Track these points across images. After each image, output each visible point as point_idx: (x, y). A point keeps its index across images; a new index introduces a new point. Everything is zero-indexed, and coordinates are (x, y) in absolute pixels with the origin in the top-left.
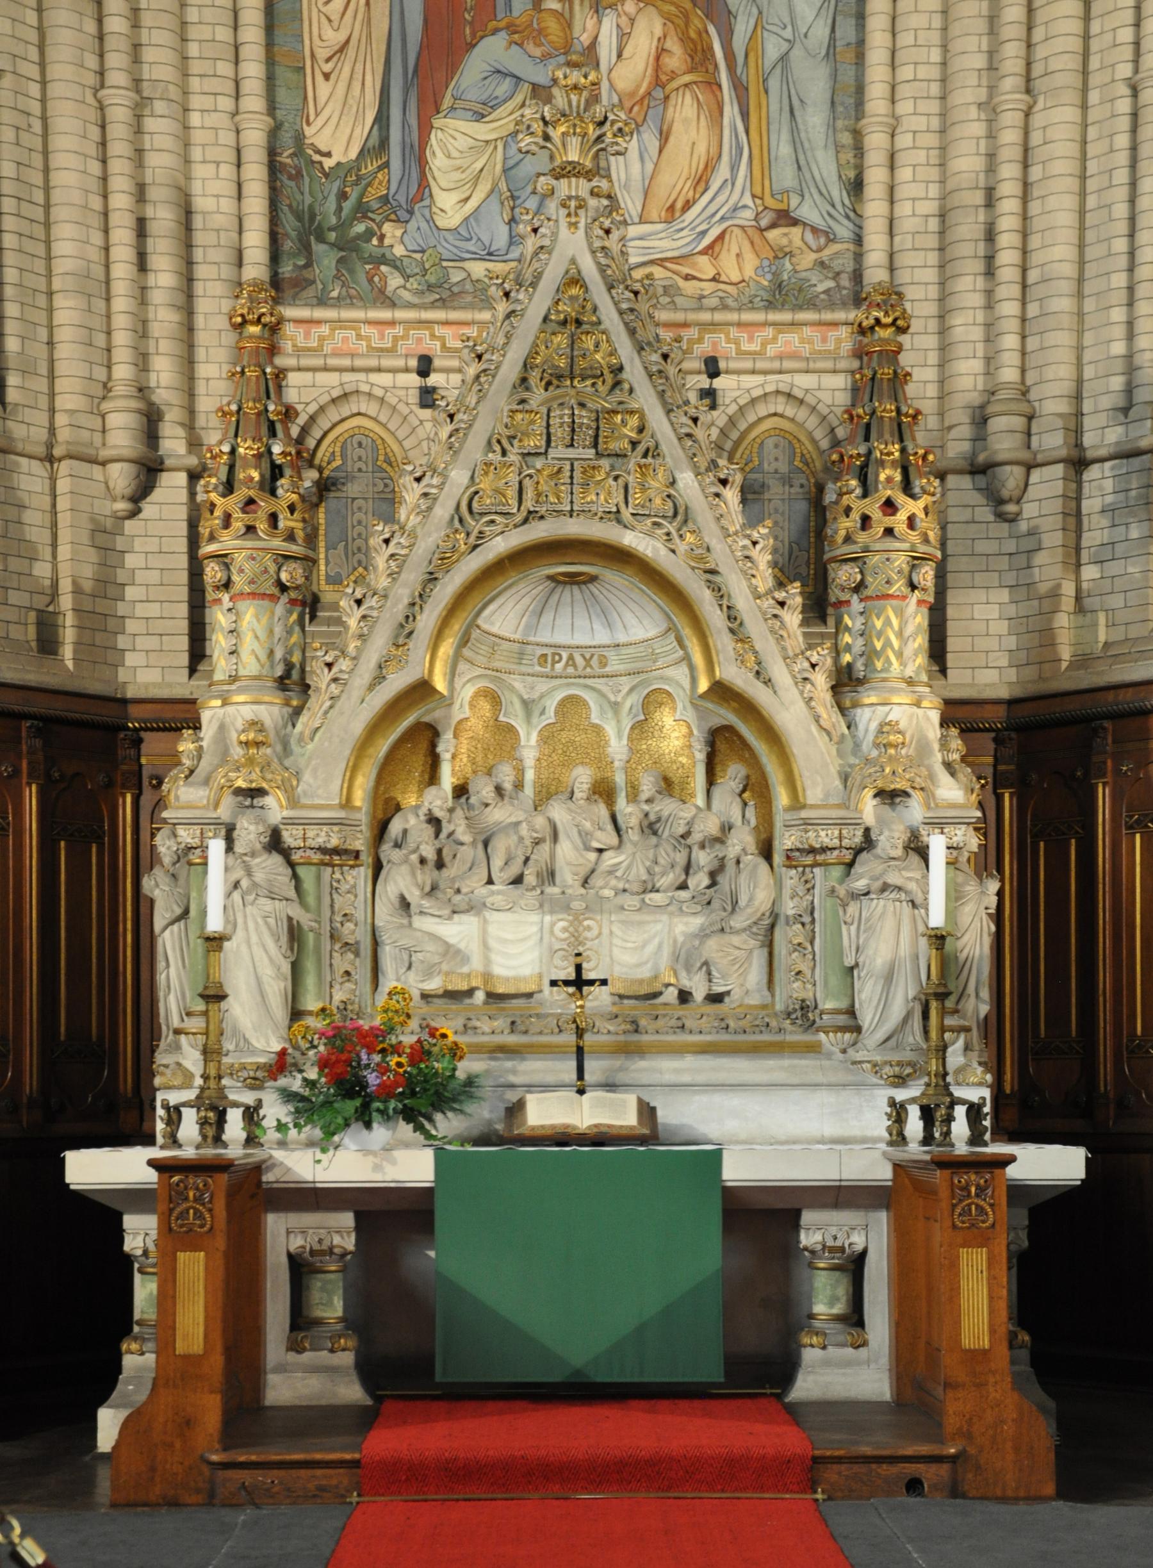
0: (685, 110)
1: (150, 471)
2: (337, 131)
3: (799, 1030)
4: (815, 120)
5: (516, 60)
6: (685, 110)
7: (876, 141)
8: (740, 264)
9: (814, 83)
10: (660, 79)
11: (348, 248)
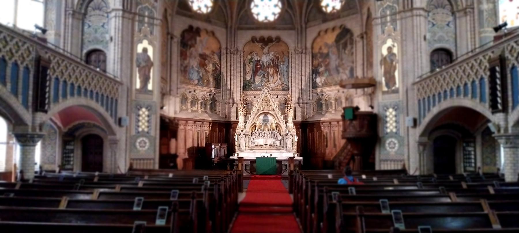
0: (275, 76)
1: (234, 104)
2: (248, 78)
3: (283, 147)
4: (286, 76)
5: (262, 72)
6: (275, 76)
7: (290, 78)
8: (280, 87)
9: (285, 74)
10: (273, 73)
11: (249, 86)
